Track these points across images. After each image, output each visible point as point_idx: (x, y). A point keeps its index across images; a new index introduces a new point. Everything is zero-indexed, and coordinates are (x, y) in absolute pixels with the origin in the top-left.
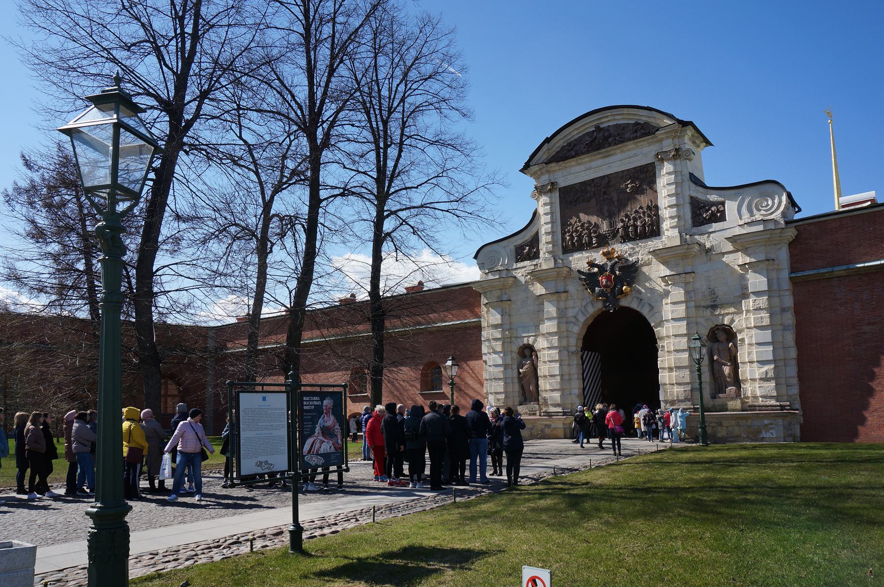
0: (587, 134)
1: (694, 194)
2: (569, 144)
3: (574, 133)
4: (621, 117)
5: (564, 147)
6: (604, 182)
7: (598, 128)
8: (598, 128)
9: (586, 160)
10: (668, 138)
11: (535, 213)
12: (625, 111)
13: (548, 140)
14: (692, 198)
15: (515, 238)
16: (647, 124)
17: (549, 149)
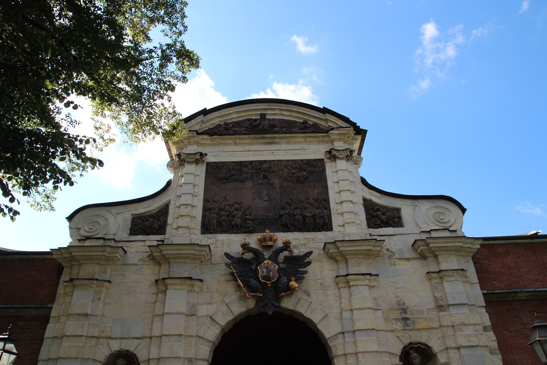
0: (248, 120)
1: (368, 197)
2: (226, 124)
3: (234, 116)
4: (289, 113)
5: (220, 125)
6: (265, 166)
7: (263, 116)
8: (263, 116)
9: (246, 141)
10: (340, 140)
11: (169, 183)
12: (295, 108)
13: (205, 112)
14: (364, 200)
15: (135, 206)
16: (315, 125)
17: (202, 122)
